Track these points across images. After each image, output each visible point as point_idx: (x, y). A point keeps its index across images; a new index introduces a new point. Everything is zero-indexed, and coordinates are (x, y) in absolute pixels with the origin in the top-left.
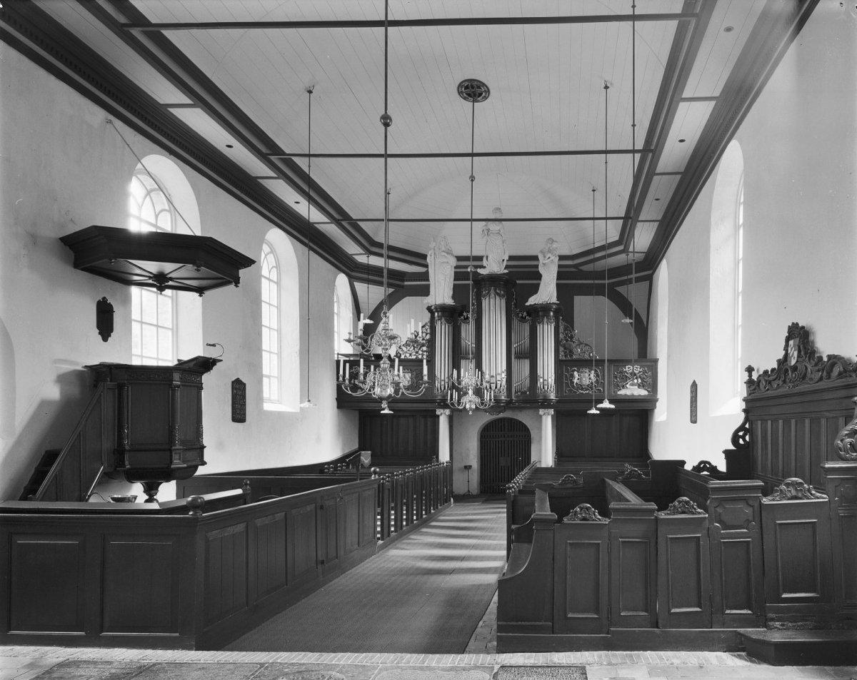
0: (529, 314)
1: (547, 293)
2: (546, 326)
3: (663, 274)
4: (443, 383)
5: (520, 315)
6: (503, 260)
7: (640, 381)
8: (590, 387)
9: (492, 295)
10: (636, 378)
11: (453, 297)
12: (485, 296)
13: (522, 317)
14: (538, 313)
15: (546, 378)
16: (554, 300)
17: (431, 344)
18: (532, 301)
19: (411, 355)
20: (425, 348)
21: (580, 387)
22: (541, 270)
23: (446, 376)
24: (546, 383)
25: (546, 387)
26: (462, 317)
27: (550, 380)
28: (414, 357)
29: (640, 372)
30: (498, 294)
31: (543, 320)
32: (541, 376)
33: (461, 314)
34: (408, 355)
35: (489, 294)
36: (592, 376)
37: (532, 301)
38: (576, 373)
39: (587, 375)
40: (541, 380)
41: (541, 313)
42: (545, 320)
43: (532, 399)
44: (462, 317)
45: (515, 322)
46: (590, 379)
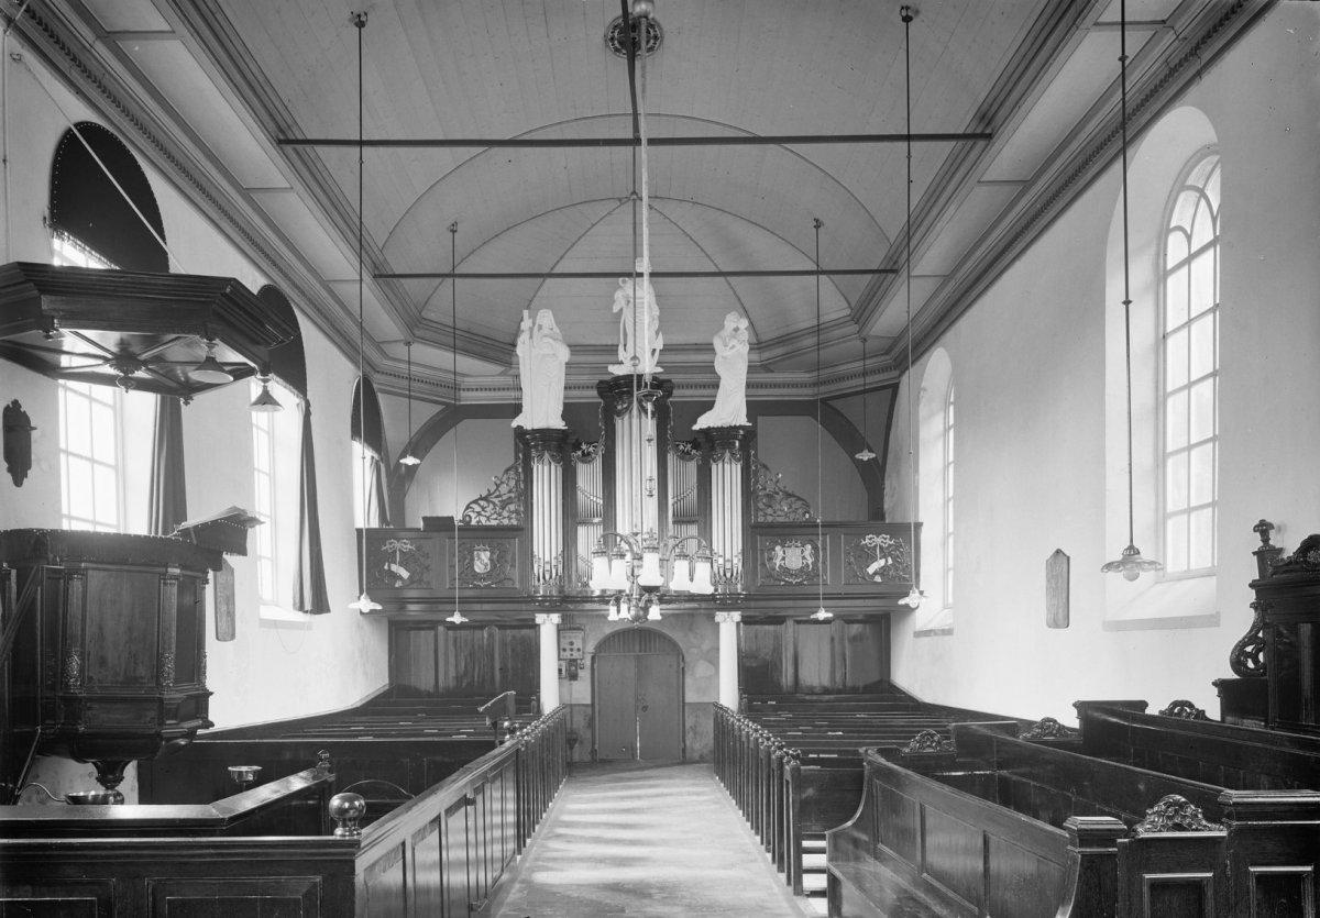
1: (729, 409)
2: (727, 466)
3: (937, 367)
4: (547, 567)
6: (654, 350)
7: (890, 561)
11: (564, 417)
12: (620, 414)
14: (713, 444)
15: (728, 556)
16: (742, 420)
17: (525, 495)
18: (703, 422)
19: (488, 518)
20: (512, 507)
21: (786, 571)
22: (719, 368)
23: (554, 555)
25: (728, 575)
26: (580, 453)
27: (735, 561)
28: (494, 523)
29: (890, 546)
31: (723, 454)
32: (721, 553)
33: (577, 446)
34: (483, 520)
37: (703, 422)
38: (778, 548)
40: (721, 561)
42: (727, 455)
44: (580, 453)
45: (671, 458)
46: (804, 558)
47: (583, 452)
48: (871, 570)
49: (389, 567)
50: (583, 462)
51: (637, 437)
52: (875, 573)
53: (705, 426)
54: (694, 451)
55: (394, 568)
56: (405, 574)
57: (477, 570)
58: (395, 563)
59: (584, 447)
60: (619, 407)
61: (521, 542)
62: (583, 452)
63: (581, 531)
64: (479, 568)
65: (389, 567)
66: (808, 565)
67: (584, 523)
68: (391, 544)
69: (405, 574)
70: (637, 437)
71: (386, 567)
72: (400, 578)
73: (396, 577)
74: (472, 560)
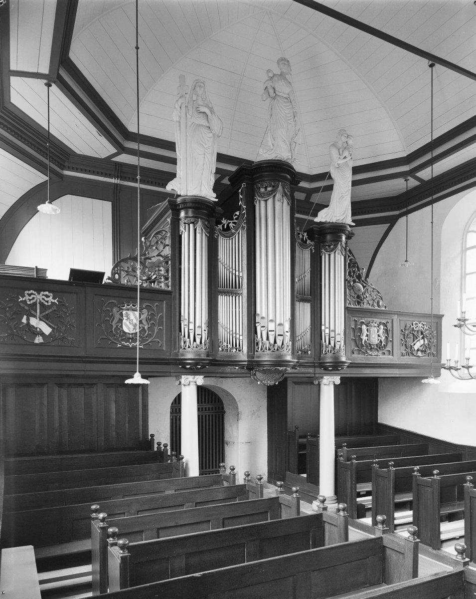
0: (311, 237)
1: (338, 211)
5: (301, 236)
8: (380, 347)
9: (278, 196)
10: (423, 338)
11: (215, 190)
12: (264, 196)
13: (302, 240)
15: (332, 328)
24: (332, 334)
26: (220, 227)
30: (286, 195)
35: (273, 193)
36: (381, 331)
39: (376, 329)
41: (329, 237)
43: (317, 359)
46: (379, 336)
47: (223, 226)
48: (416, 347)
49: (28, 319)
50: (225, 236)
51: (274, 217)
52: (418, 350)
53: (323, 220)
54: (308, 241)
55: (34, 322)
56: (47, 330)
57: (125, 329)
58: (35, 316)
59: (224, 221)
60: (262, 190)
61: (169, 307)
62: (223, 226)
63: (222, 300)
64: (129, 329)
65: (28, 319)
66: (381, 342)
67: (226, 293)
68: (30, 295)
69: (47, 330)
70: (274, 217)
71: (24, 320)
72: (42, 334)
73: (36, 332)
74: (121, 321)
